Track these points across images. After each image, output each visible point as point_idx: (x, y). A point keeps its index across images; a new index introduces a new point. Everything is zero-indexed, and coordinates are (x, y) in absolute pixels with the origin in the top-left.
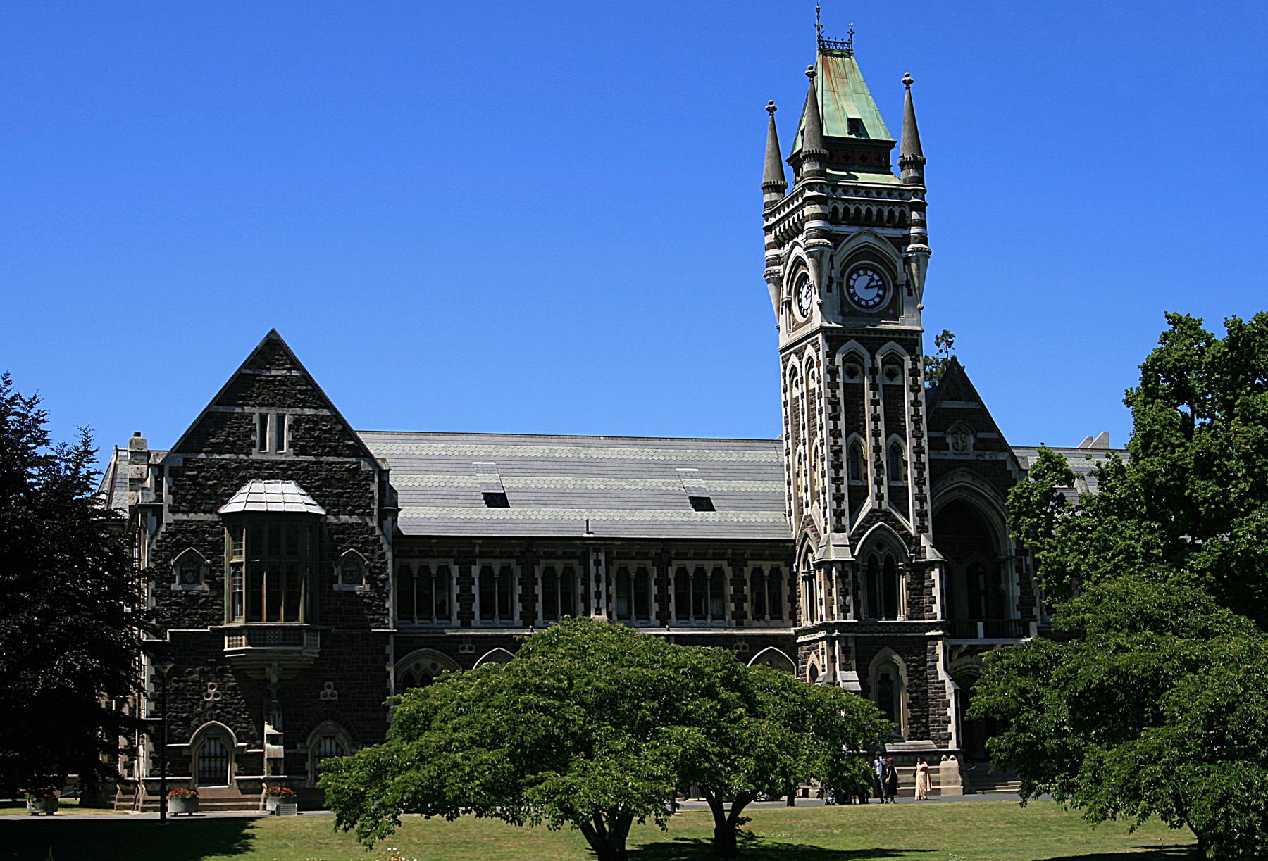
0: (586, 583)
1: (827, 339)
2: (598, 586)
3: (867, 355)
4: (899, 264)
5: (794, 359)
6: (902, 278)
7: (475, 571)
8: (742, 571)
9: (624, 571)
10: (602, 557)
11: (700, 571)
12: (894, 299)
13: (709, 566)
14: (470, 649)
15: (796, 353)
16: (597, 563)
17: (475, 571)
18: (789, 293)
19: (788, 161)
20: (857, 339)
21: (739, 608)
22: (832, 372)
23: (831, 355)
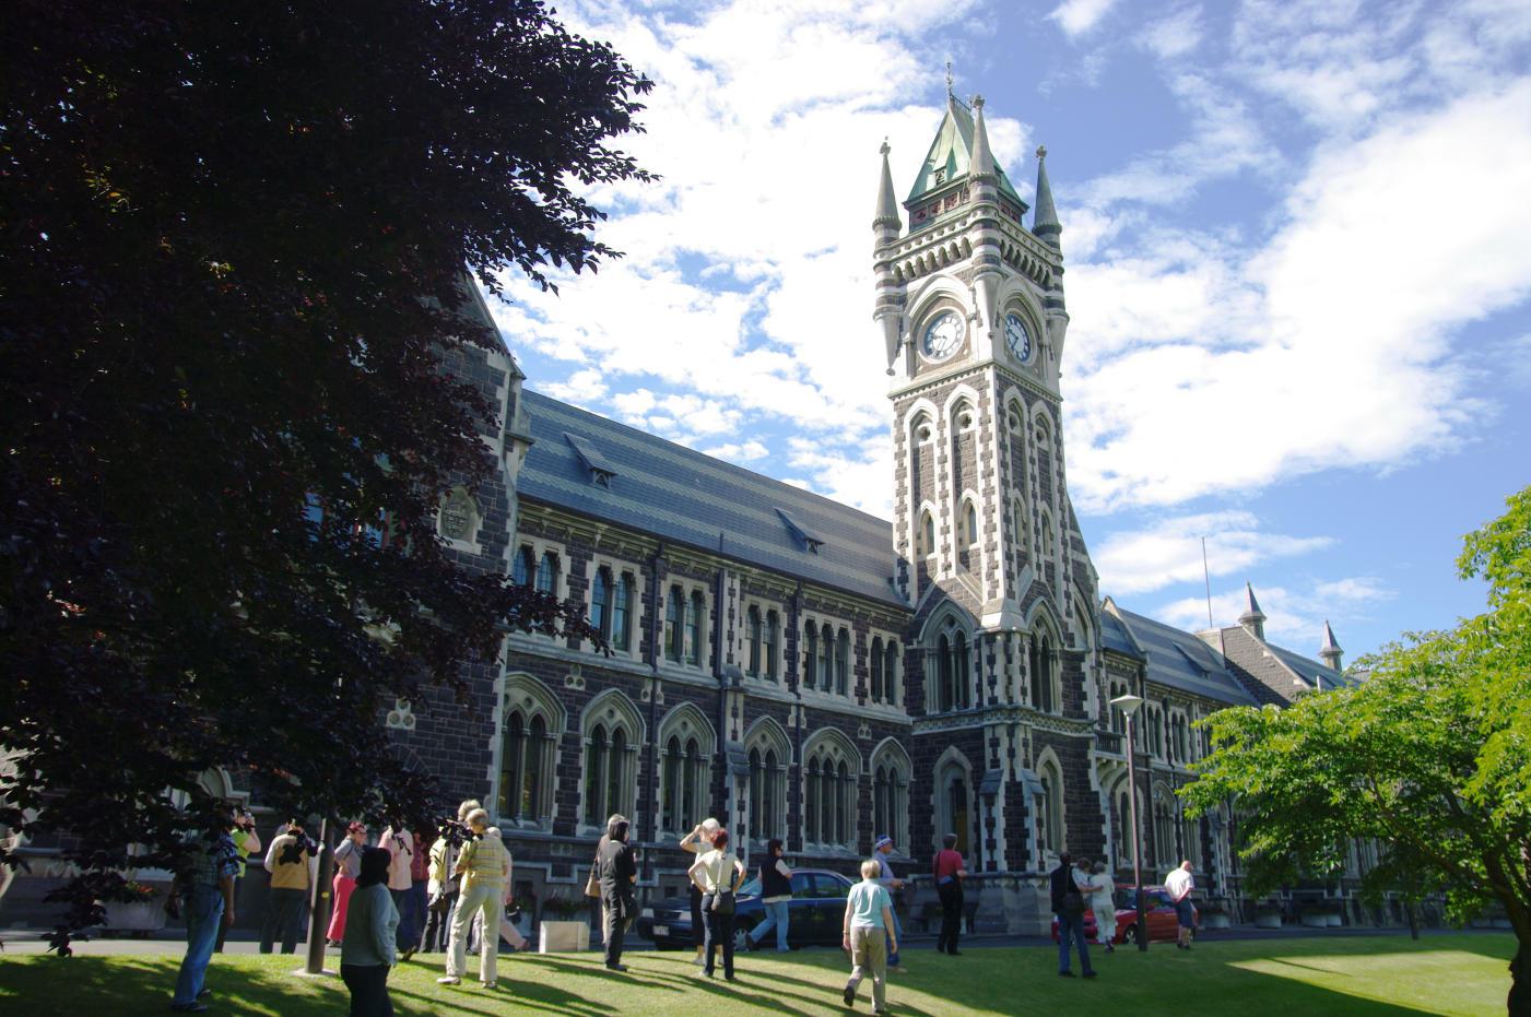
0: (716, 616)
1: (998, 377)
2: (731, 624)
3: (1025, 407)
4: (1044, 324)
5: (923, 403)
6: (1046, 340)
7: (591, 569)
8: (864, 637)
9: (753, 610)
10: (737, 585)
11: (827, 628)
12: (1039, 360)
13: (837, 624)
14: (580, 683)
15: (934, 396)
16: (732, 592)
17: (591, 569)
18: (914, 335)
19: (908, 205)
20: (1019, 387)
21: (861, 683)
22: (1000, 412)
23: (1000, 394)
